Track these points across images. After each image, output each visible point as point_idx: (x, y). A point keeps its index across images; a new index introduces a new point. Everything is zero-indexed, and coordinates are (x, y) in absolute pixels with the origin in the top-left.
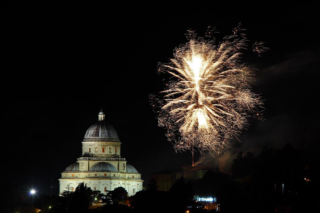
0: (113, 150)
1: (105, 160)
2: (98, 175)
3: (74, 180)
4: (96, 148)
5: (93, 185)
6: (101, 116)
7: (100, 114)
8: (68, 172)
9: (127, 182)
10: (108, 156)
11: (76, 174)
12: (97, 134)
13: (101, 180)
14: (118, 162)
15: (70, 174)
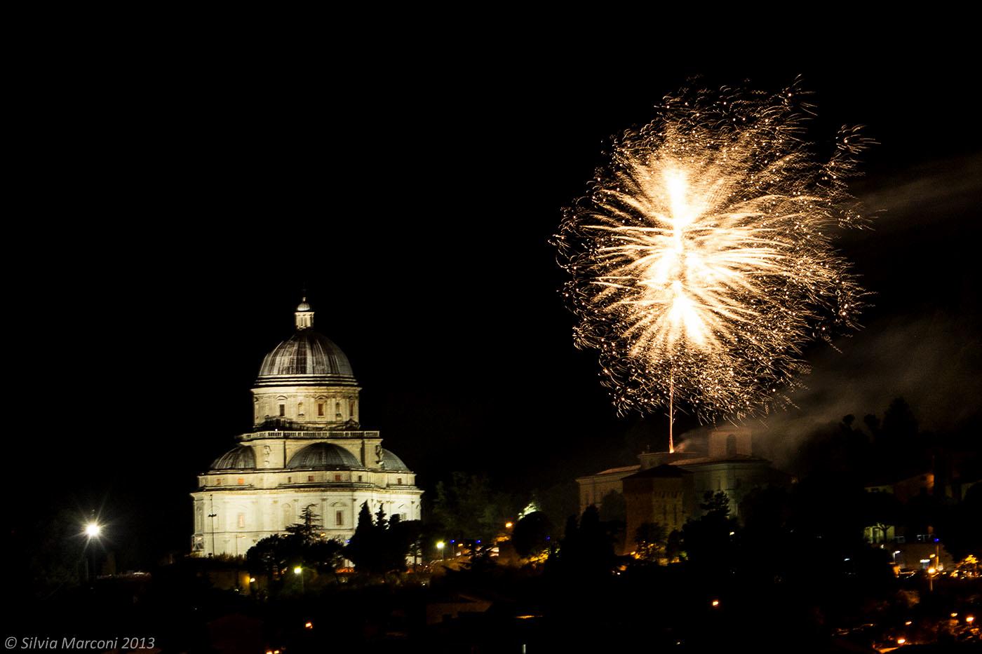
0: (344, 410)
1: (328, 438)
2: (316, 480)
3: (243, 494)
4: (300, 404)
6: (304, 317)
7: (299, 309)
8: (223, 471)
10: (334, 426)
11: (249, 478)
12: (300, 366)
13: (328, 493)
14: (360, 441)
15: (231, 479)
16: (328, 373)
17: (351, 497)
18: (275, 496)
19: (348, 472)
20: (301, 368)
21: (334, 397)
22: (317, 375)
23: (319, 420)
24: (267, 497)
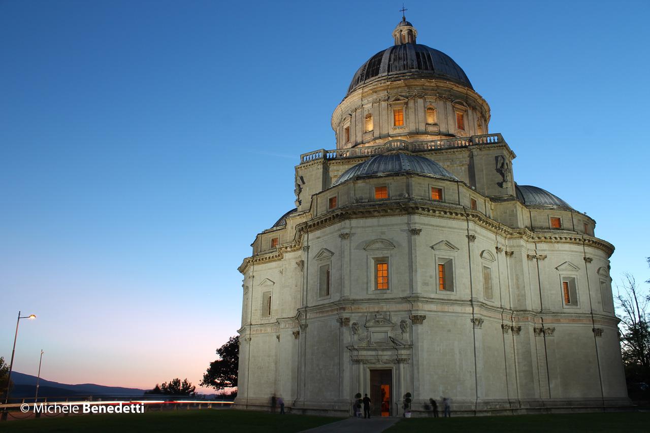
3: (271, 260)
5: (319, 256)
9: (526, 246)
13: (354, 222)
16: (413, 68)
18: (300, 252)
19: (402, 180)
20: (373, 71)
21: (421, 97)
22: (394, 73)
23: (398, 131)
24: (291, 258)
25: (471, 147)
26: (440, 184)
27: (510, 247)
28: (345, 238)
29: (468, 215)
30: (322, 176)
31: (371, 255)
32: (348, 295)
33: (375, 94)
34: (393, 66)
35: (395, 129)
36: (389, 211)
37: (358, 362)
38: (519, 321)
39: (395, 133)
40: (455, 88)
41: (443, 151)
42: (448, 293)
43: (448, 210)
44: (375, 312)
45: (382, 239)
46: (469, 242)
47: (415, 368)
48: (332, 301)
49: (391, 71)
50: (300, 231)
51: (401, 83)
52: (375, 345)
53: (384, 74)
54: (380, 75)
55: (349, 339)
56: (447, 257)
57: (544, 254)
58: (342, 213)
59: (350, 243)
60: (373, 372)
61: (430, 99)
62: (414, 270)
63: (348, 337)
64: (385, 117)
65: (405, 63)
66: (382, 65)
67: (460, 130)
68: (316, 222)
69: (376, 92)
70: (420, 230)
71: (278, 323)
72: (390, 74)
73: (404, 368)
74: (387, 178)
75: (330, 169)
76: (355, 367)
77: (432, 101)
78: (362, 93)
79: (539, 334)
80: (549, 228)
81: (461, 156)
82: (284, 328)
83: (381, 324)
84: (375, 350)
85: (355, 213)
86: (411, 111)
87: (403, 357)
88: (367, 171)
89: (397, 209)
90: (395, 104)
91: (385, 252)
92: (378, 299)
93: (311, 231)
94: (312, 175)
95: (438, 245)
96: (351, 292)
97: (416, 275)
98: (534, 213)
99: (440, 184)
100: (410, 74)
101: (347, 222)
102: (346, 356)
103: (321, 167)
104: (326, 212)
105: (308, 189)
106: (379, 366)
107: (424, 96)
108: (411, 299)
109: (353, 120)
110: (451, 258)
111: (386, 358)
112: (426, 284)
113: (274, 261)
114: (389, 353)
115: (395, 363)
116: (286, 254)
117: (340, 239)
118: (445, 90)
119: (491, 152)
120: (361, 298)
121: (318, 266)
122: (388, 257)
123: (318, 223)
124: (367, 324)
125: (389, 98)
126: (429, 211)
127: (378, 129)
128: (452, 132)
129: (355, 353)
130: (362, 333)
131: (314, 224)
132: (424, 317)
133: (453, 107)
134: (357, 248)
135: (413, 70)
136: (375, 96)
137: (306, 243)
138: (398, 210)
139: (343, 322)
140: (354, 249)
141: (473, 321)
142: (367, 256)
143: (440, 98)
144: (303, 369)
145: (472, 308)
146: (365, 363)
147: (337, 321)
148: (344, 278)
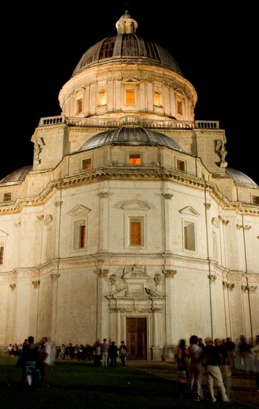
5: (74, 211)
9: (236, 217)
13: (112, 183)
16: (143, 56)
17: (159, 192)
18: (41, 208)
19: (154, 150)
20: (106, 52)
21: (150, 81)
22: (126, 57)
23: (130, 108)
24: (30, 213)
25: (196, 130)
26: (183, 158)
27: (227, 217)
28: (104, 197)
29: (207, 186)
30: (62, 140)
31: (127, 214)
32: (106, 248)
33: (109, 73)
34: (126, 51)
35: (127, 106)
36: (145, 176)
37: (116, 310)
38: (232, 280)
39: (126, 109)
40: (177, 78)
41: (171, 130)
42: (191, 251)
43: (193, 181)
44: (131, 265)
45: (139, 201)
46: (206, 210)
47: (168, 317)
48: (88, 253)
49: (124, 55)
50: (52, 187)
51: (135, 67)
52: (131, 295)
53: (118, 57)
54: (113, 57)
55: (108, 289)
56: (190, 221)
57: (249, 225)
58: (103, 174)
59: (109, 202)
60: (129, 319)
61: (158, 84)
62: (166, 230)
63: (106, 287)
64: (118, 95)
65: (136, 50)
66: (115, 49)
67: (179, 115)
68: (73, 180)
69: (111, 71)
70: (172, 196)
71: (15, 272)
72: (123, 57)
73: (158, 317)
74: (141, 147)
75: (70, 134)
76: (113, 315)
77: (159, 86)
78: (98, 71)
79: (245, 291)
80: (251, 204)
81: (185, 136)
82: (22, 278)
83: (137, 276)
84: (133, 300)
85: (114, 175)
86: (142, 93)
87: (158, 307)
88: (118, 139)
89: (153, 175)
90: (128, 85)
91: (141, 212)
92: (135, 254)
93: (65, 188)
94: (52, 138)
95: (185, 210)
96: (110, 245)
97: (168, 234)
98: (240, 190)
99: (183, 158)
100: (142, 60)
101: (106, 182)
102: (105, 305)
103: (62, 131)
104: (78, 172)
105: (48, 150)
106: (135, 314)
107: (153, 81)
108: (164, 255)
109: (87, 93)
110: (193, 222)
111: (142, 307)
112: (175, 243)
113: (9, 213)
114: (144, 303)
115: (149, 312)
116: (27, 208)
117: (98, 198)
118: (169, 79)
119: (211, 136)
120: (121, 252)
121: (72, 221)
122: (143, 217)
123: (75, 181)
124: (125, 276)
125: (122, 78)
126: (179, 179)
127: (111, 104)
128: (174, 115)
129: (113, 302)
130: (119, 283)
131: (79, 180)
132: (175, 272)
133: (175, 94)
134: (115, 206)
135: (143, 57)
136: (110, 75)
137: (60, 199)
138: (154, 176)
139: (101, 273)
140: (112, 208)
141: (209, 277)
142: (124, 214)
143: (166, 84)
144: (54, 316)
145: (208, 266)
146: (122, 312)
147: (95, 272)
148: (103, 233)
